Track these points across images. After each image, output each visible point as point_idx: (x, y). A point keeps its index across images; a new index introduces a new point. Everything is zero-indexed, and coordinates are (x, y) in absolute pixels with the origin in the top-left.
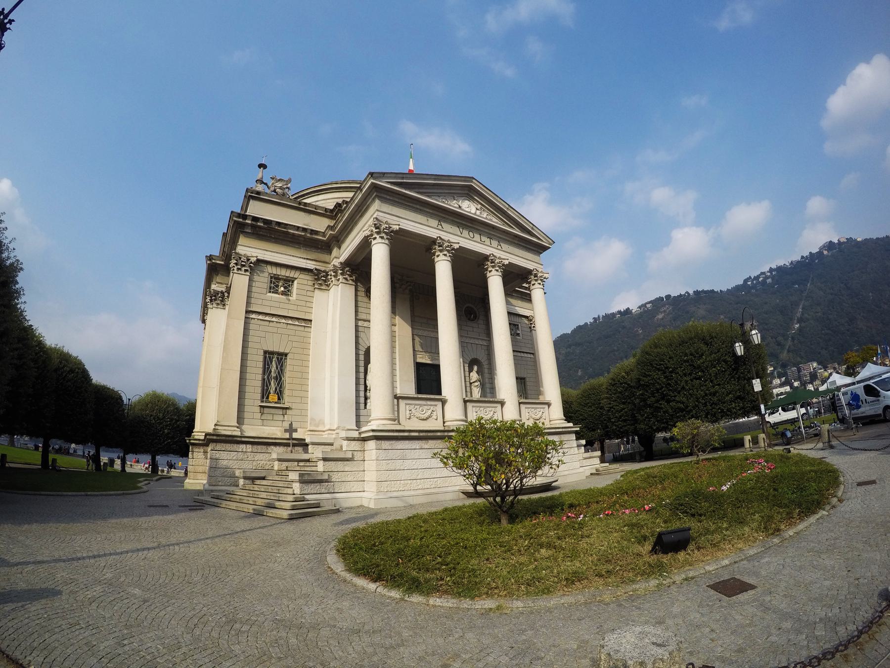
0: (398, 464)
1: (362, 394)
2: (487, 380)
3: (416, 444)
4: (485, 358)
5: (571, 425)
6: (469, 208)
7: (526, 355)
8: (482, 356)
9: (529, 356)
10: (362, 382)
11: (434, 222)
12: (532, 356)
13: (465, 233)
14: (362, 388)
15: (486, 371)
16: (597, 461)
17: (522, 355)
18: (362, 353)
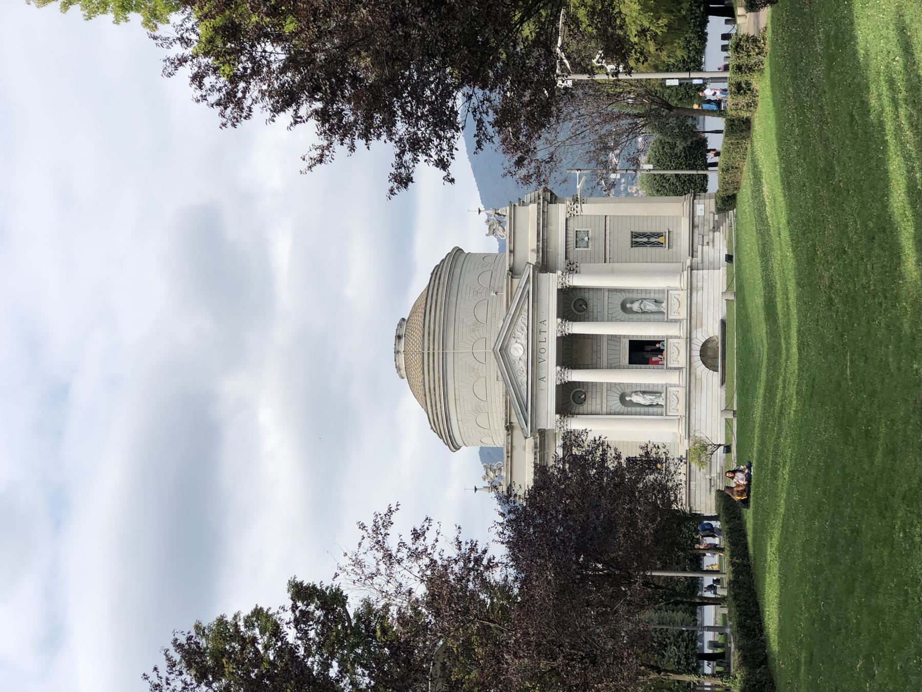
0: (703, 423)
1: (655, 409)
2: (639, 296)
3: (693, 411)
4: (619, 294)
5: (685, 272)
6: (518, 351)
7: (608, 227)
8: (618, 299)
9: (608, 222)
10: (646, 409)
11: (543, 384)
12: (608, 218)
13: (543, 356)
14: (651, 410)
15: (630, 296)
16: (717, 234)
17: (608, 232)
18: (626, 409)
